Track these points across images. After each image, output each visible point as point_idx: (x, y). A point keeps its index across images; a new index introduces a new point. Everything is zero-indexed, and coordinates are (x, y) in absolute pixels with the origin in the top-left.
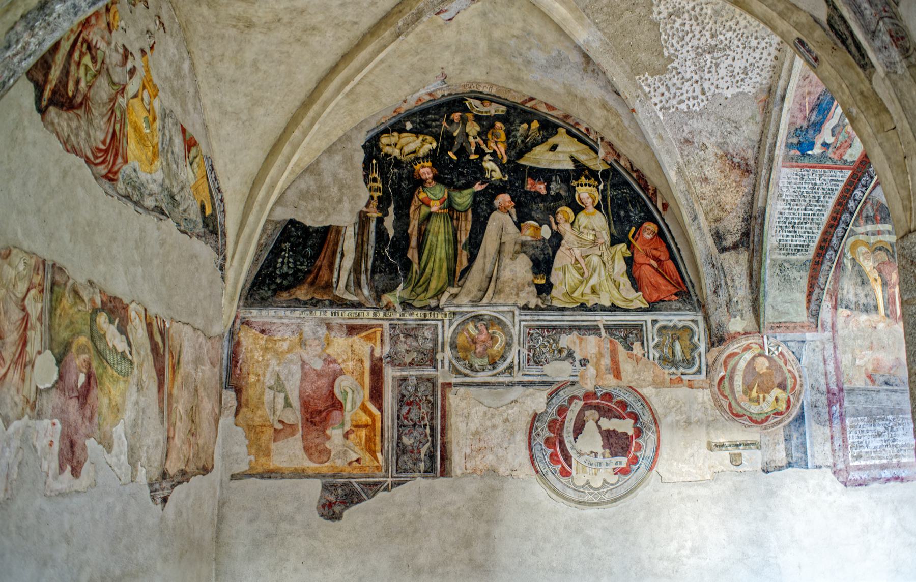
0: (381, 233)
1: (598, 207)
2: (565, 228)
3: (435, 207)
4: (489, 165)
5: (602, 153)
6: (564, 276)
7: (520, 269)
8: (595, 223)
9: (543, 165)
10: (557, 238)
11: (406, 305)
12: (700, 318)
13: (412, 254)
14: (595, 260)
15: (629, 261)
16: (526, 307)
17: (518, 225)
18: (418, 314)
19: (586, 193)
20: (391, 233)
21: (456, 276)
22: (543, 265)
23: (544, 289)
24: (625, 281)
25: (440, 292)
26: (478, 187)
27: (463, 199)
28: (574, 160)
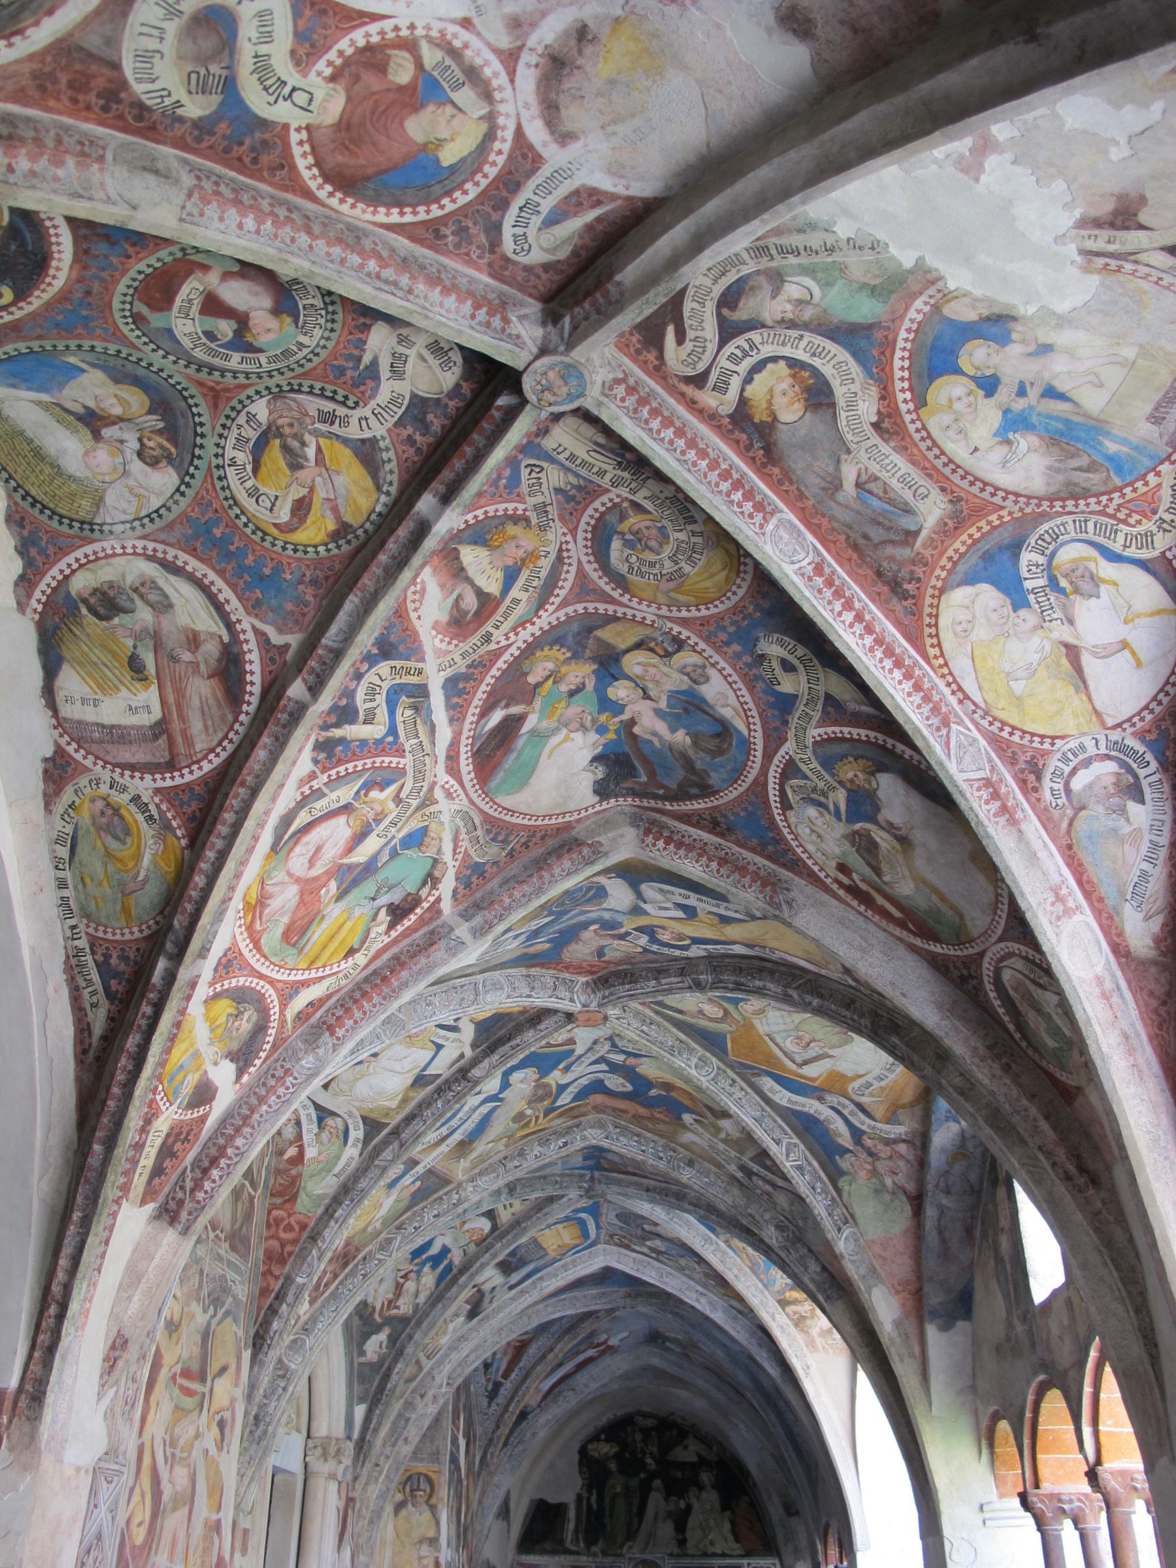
0: (589, 1506)
1: (713, 1487)
2: (693, 1501)
3: (618, 1490)
4: (649, 1461)
5: (715, 1449)
6: (693, 1534)
7: (667, 1529)
8: (711, 1497)
9: (680, 1459)
10: (689, 1509)
11: (605, 1553)
12: (777, 1562)
13: (607, 1520)
14: (712, 1522)
15: (733, 1523)
16: (671, 1555)
17: (666, 1499)
18: (610, 1559)
19: (705, 1477)
20: (595, 1507)
21: (631, 1535)
22: (681, 1526)
23: (682, 1543)
24: (730, 1537)
25: (622, 1546)
26: (643, 1476)
27: (634, 1483)
28: (699, 1455)
